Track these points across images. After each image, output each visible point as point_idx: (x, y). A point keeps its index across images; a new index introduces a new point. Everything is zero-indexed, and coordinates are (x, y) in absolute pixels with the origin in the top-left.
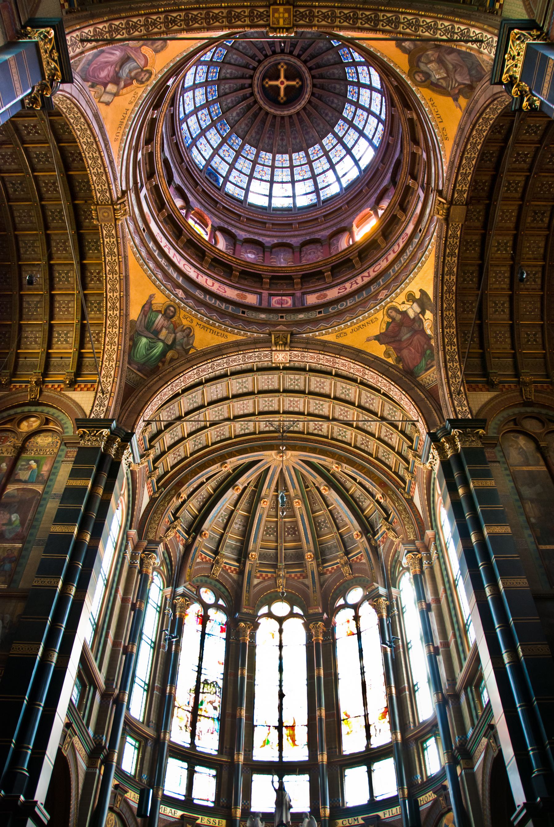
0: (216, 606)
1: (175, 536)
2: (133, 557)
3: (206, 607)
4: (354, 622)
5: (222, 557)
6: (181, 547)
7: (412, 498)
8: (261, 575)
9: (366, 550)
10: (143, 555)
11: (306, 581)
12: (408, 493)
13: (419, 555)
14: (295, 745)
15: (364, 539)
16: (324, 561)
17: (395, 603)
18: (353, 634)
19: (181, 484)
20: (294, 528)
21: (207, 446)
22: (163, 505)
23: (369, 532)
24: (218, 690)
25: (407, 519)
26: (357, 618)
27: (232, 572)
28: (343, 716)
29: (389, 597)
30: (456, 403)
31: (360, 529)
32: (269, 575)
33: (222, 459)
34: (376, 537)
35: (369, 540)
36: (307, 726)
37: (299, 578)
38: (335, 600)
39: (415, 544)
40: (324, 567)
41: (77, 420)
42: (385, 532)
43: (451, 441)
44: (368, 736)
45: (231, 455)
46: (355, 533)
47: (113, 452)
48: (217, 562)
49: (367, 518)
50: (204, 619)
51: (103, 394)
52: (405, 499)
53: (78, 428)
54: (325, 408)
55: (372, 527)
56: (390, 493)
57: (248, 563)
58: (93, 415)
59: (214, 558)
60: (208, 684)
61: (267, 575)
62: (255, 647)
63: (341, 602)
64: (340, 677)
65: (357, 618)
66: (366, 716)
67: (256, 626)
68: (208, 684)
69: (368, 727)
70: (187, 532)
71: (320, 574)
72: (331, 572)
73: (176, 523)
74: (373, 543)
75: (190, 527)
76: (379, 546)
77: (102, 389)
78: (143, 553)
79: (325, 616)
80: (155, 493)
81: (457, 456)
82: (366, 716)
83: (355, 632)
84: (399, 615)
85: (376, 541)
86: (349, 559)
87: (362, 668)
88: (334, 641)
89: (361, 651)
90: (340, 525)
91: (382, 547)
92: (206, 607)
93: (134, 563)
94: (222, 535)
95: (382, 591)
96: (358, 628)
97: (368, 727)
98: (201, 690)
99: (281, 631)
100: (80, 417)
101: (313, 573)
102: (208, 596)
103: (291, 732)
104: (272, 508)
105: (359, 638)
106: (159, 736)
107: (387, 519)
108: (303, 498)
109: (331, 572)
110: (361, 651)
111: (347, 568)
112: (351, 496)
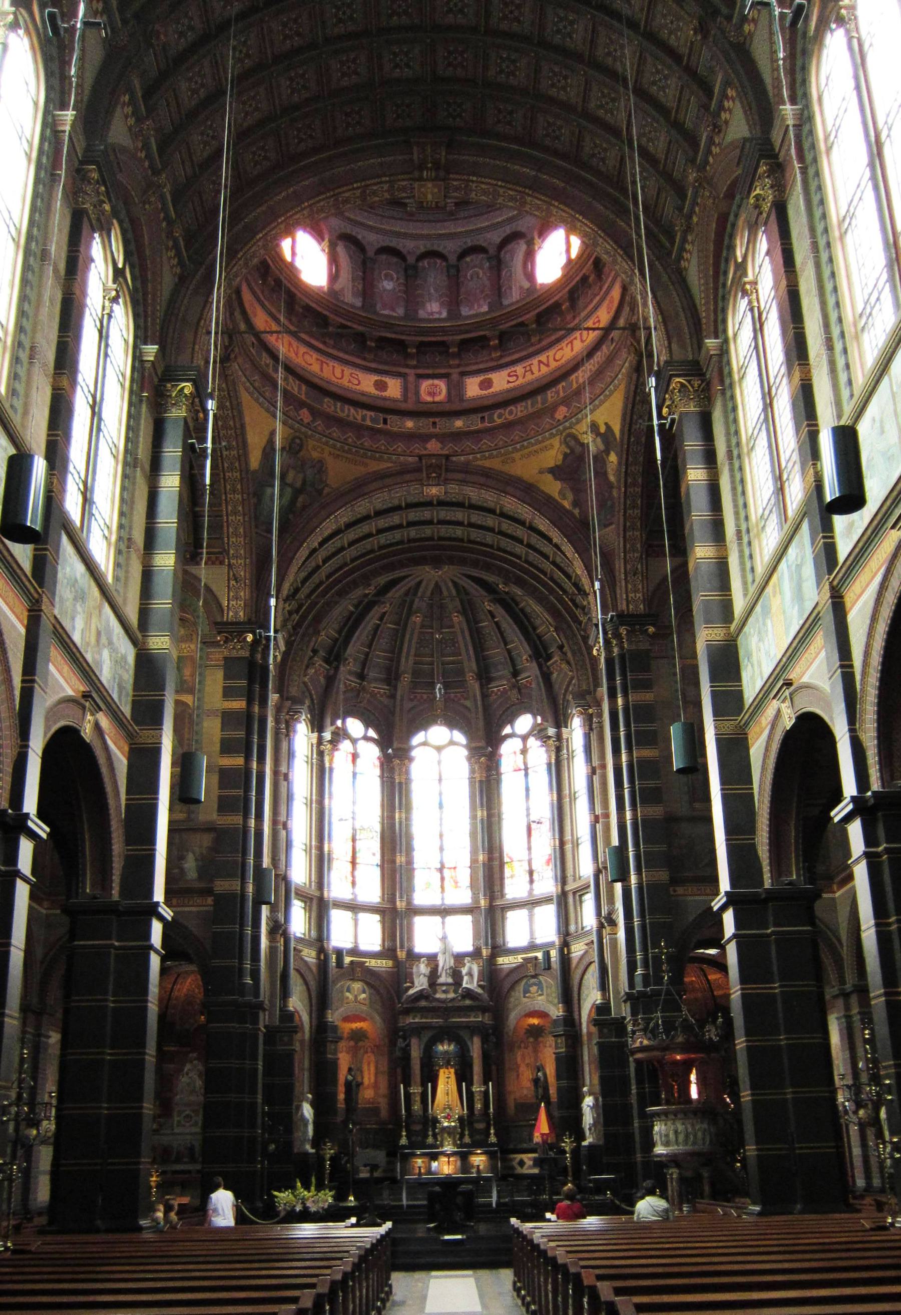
0: (366, 738)
1: (316, 671)
2: (277, 721)
3: (354, 741)
4: (522, 756)
5: (369, 683)
6: (322, 680)
7: (588, 637)
8: (416, 697)
9: (537, 677)
10: (288, 717)
11: (468, 703)
12: (585, 630)
13: (590, 711)
14: (457, 887)
15: (535, 664)
16: (490, 680)
17: (565, 744)
18: (520, 770)
19: (318, 619)
20: (453, 640)
21: (346, 564)
22: (302, 650)
23: (541, 656)
24: (375, 834)
25: (581, 663)
26: (524, 751)
27: (382, 696)
28: (506, 859)
29: (559, 737)
30: (630, 586)
31: (530, 652)
32: (425, 696)
33: (366, 580)
34: (549, 663)
35: (540, 666)
36: (470, 867)
37: (460, 699)
38: (501, 727)
39: (585, 699)
40: (488, 688)
41: (216, 623)
42: (556, 661)
43: (617, 636)
44: (531, 881)
45: (376, 573)
46: (524, 657)
47: (259, 656)
48: (364, 689)
49: (539, 637)
50: (355, 756)
51: (237, 582)
52: (581, 636)
53: (219, 633)
54: (490, 521)
55: (546, 649)
56: (565, 626)
57: (400, 686)
58: (231, 614)
59: (360, 684)
60: (364, 829)
61: (422, 697)
62: (410, 783)
63: (507, 730)
64: (504, 816)
65: (524, 751)
66: (530, 862)
67: (411, 760)
68: (364, 829)
69: (531, 873)
70: (327, 661)
71: (484, 696)
72: (496, 694)
73: (316, 659)
74: (545, 669)
75: (330, 652)
76: (552, 673)
77: (234, 575)
78: (287, 714)
79: (490, 749)
80: (290, 636)
81: (622, 657)
82: (530, 862)
83: (523, 767)
84: (568, 759)
85: (548, 668)
86: (517, 681)
87: (528, 809)
88: (499, 774)
89: (527, 790)
90: (508, 640)
91: (555, 675)
92: (354, 741)
93: (280, 729)
94: (367, 655)
95: (551, 731)
96: (525, 764)
97: (531, 873)
98: (357, 837)
99: (439, 762)
100: (219, 620)
101: (475, 696)
102: (355, 726)
103: (453, 874)
104: (426, 617)
105: (526, 775)
106: (322, 894)
107: (561, 647)
108: (463, 608)
109: (496, 694)
110: (527, 790)
111: (515, 691)
112: (522, 610)
